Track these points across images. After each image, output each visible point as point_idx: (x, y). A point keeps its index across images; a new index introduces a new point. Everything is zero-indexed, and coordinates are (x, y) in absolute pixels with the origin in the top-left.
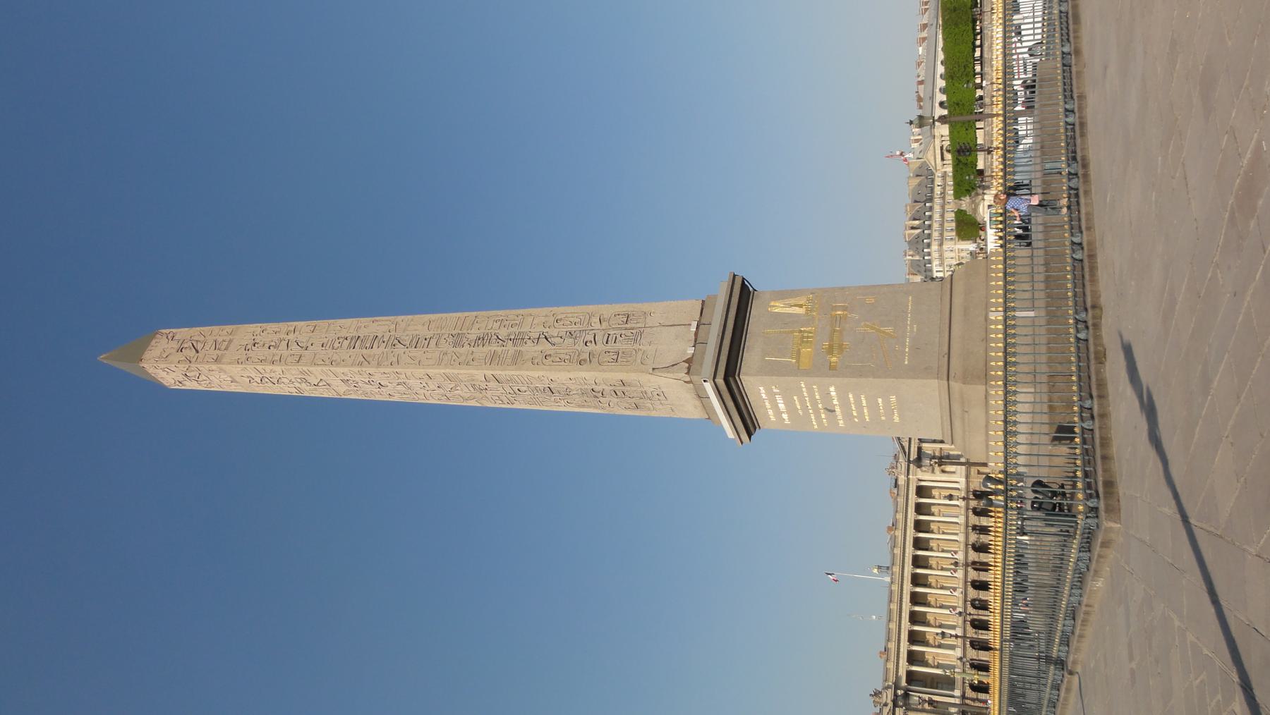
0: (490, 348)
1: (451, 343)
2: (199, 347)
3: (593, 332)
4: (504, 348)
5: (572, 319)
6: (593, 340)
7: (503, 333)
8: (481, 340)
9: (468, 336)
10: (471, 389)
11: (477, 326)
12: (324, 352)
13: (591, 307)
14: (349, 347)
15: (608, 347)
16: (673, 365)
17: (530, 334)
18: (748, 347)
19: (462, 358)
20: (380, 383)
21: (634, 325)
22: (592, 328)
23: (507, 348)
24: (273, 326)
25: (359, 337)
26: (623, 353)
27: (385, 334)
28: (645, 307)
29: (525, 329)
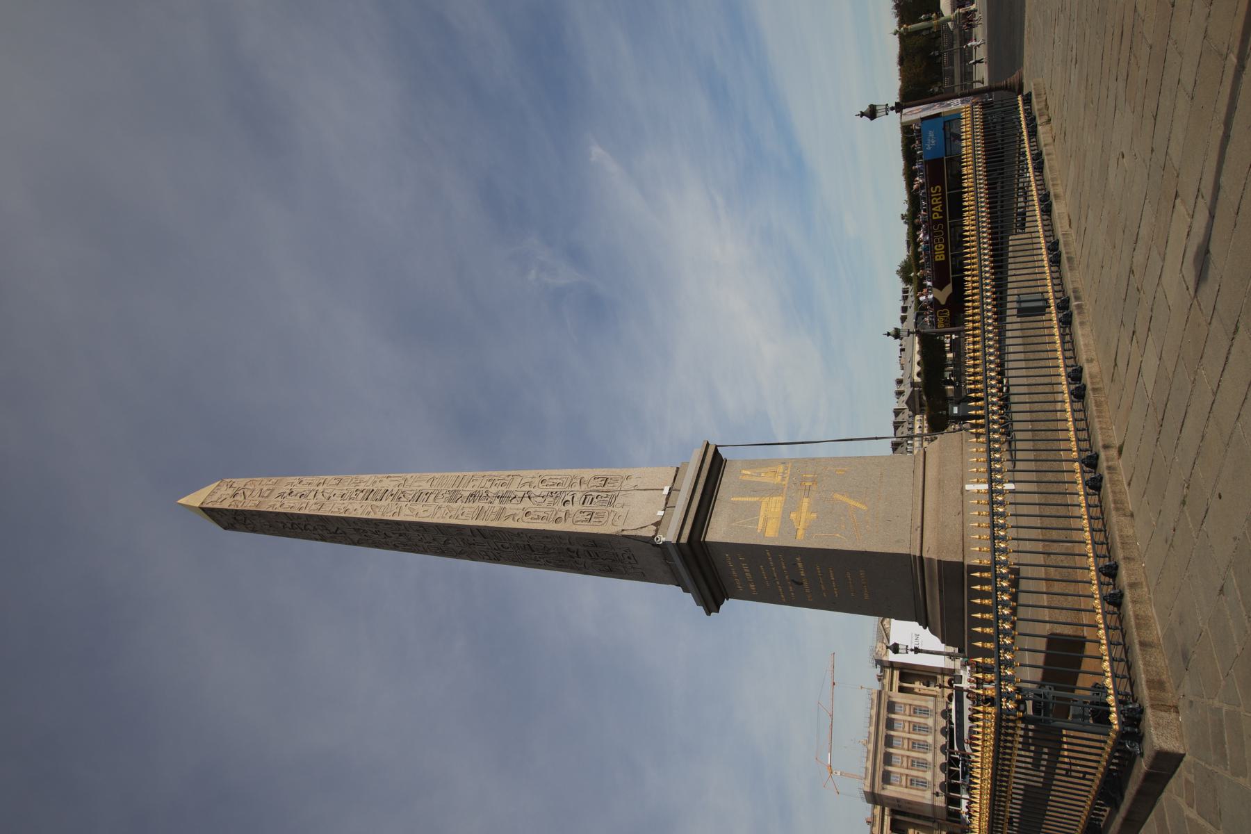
2: (248, 493)
5: (555, 481)
9: (463, 493)
10: (461, 543)
11: (472, 484)
13: (574, 470)
14: (362, 499)
16: (642, 528)
17: (516, 493)
20: (385, 534)
23: (493, 505)
25: (373, 490)
26: (597, 514)
28: (625, 472)
29: (513, 488)
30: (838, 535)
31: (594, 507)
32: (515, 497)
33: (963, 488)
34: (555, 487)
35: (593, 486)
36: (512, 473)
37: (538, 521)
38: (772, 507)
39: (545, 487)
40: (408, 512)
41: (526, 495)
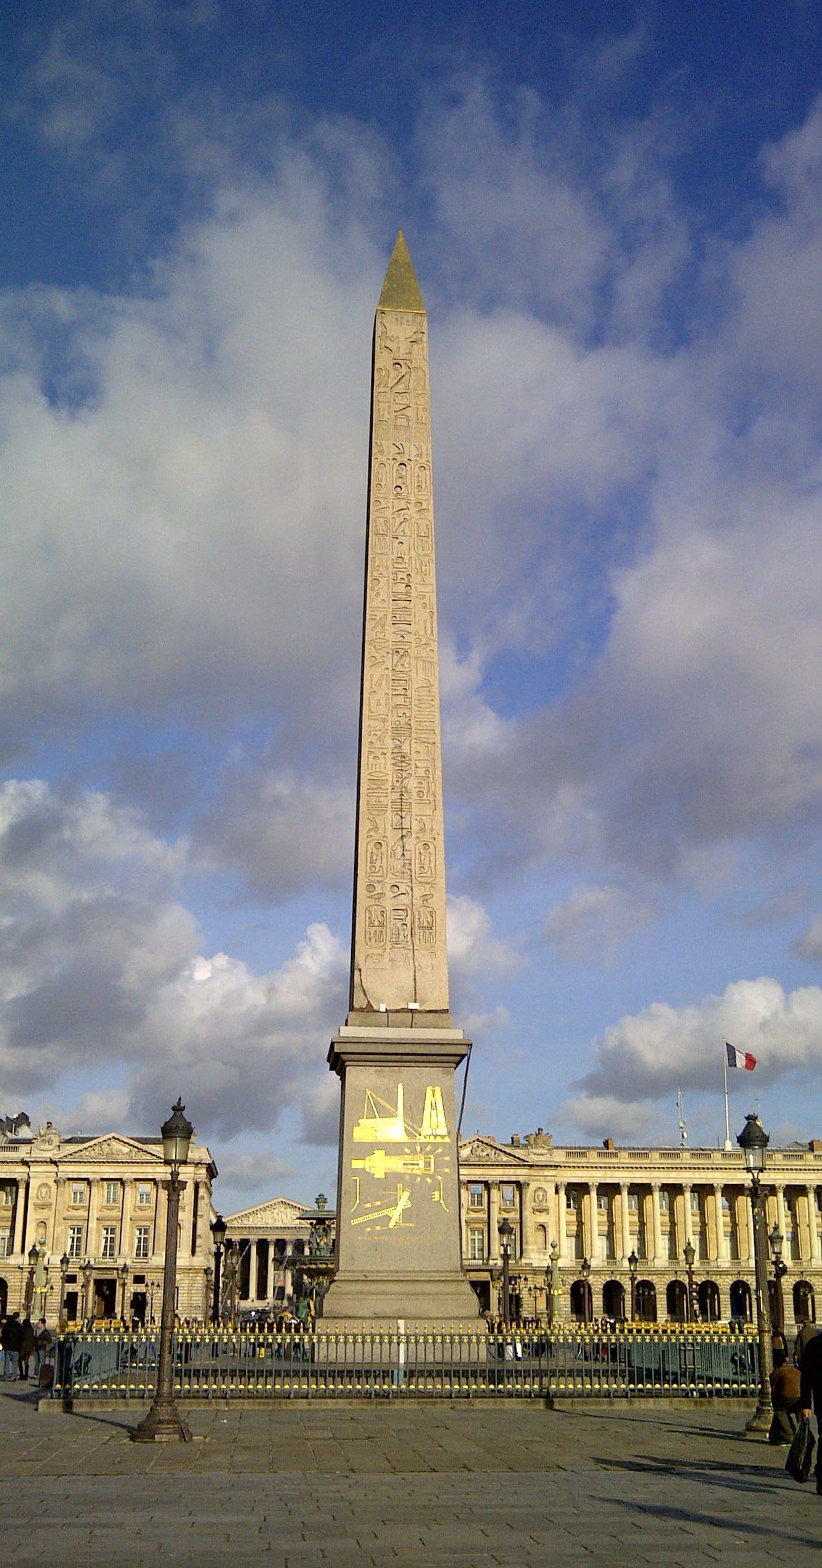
0: (390, 773)
1: (398, 723)
2: (400, 388)
3: (409, 891)
4: (389, 791)
6: (400, 893)
7: (412, 784)
8: (401, 759)
9: (407, 743)
11: (421, 748)
12: (390, 563)
13: (443, 881)
15: (390, 914)
17: (408, 817)
18: (382, 1071)
19: (377, 744)
21: (417, 937)
22: (415, 890)
24: (428, 478)
26: (381, 932)
27: (412, 635)
29: (415, 810)
30: (358, 1202)
31: (390, 924)
32: (402, 818)
33: (400, 1318)
34: (417, 866)
35: (419, 914)
36: (439, 797)
37: (369, 864)
38: (392, 1129)
39: (417, 852)
40: (376, 677)
41: (405, 832)
